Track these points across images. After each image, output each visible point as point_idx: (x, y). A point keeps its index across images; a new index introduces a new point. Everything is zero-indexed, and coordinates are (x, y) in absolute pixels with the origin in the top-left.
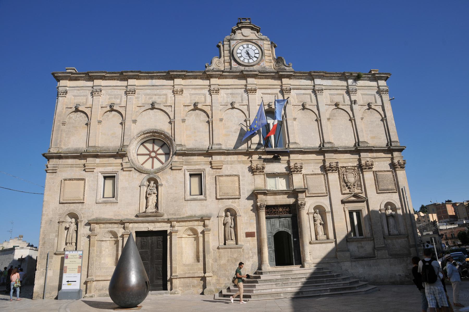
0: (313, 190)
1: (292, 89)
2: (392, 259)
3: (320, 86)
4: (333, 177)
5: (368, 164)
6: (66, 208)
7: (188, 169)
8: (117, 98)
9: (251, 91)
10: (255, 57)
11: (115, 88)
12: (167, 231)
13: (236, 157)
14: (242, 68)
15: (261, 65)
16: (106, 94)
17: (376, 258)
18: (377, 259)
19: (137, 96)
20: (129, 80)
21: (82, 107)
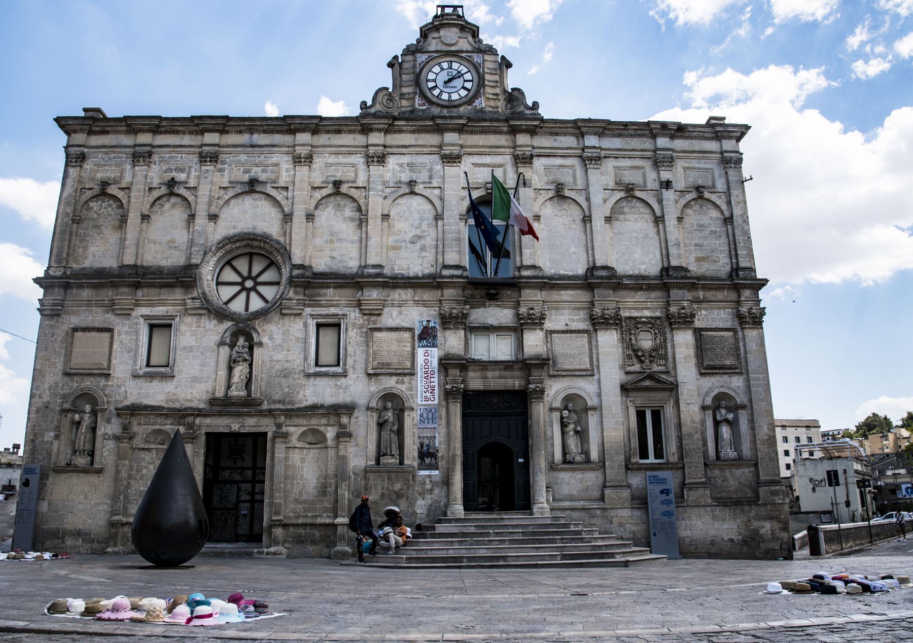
0: (565, 364)
1: (536, 155)
2: (718, 508)
3: (595, 150)
4: (609, 340)
5: (684, 313)
6: (76, 385)
7: (314, 313)
8: (182, 170)
9: (451, 158)
10: (464, 88)
11: (177, 149)
12: (266, 434)
14: (436, 111)
15: (474, 104)
16: (160, 162)
17: (685, 504)
18: (687, 506)
19: (220, 166)
20: (206, 134)
21: (113, 187)
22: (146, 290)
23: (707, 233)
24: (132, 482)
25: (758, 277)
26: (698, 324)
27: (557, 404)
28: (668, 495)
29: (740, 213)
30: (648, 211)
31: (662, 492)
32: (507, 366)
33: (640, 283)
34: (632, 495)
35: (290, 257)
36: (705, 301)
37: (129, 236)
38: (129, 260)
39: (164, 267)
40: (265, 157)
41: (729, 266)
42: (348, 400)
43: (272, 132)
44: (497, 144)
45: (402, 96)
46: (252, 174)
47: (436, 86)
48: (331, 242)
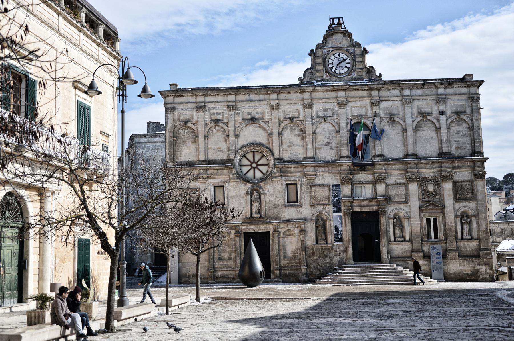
2: (462, 260)
3: (408, 97)
4: (414, 187)
10: (346, 67)
12: (269, 232)
13: (326, 168)
16: (209, 110)
19: (237, 112)
21: (189, 123)
22: (211, 171)
23: (461, 135)
24: (215, 254)
25: (485, 157)
26: (456, 178)
27: (392, 215)
28: (439, 255)
29: (477, 125)
30: (433, 126)
31: (437, 254)
32: (370, 200)
33: (428, 160)
34: (424, 254)
35: (273, 154)
36: (459, 167)
37: (200, 147)
38: (202, 158)
39: (217, 160)
40: (257, 106)
41: (471, 151)
42: (303, 217)
43: (259, 94)
44: (362, 95)
45: (317, 71)
46: (252, 115)
47: (333, 67)
48: (290, 146)
